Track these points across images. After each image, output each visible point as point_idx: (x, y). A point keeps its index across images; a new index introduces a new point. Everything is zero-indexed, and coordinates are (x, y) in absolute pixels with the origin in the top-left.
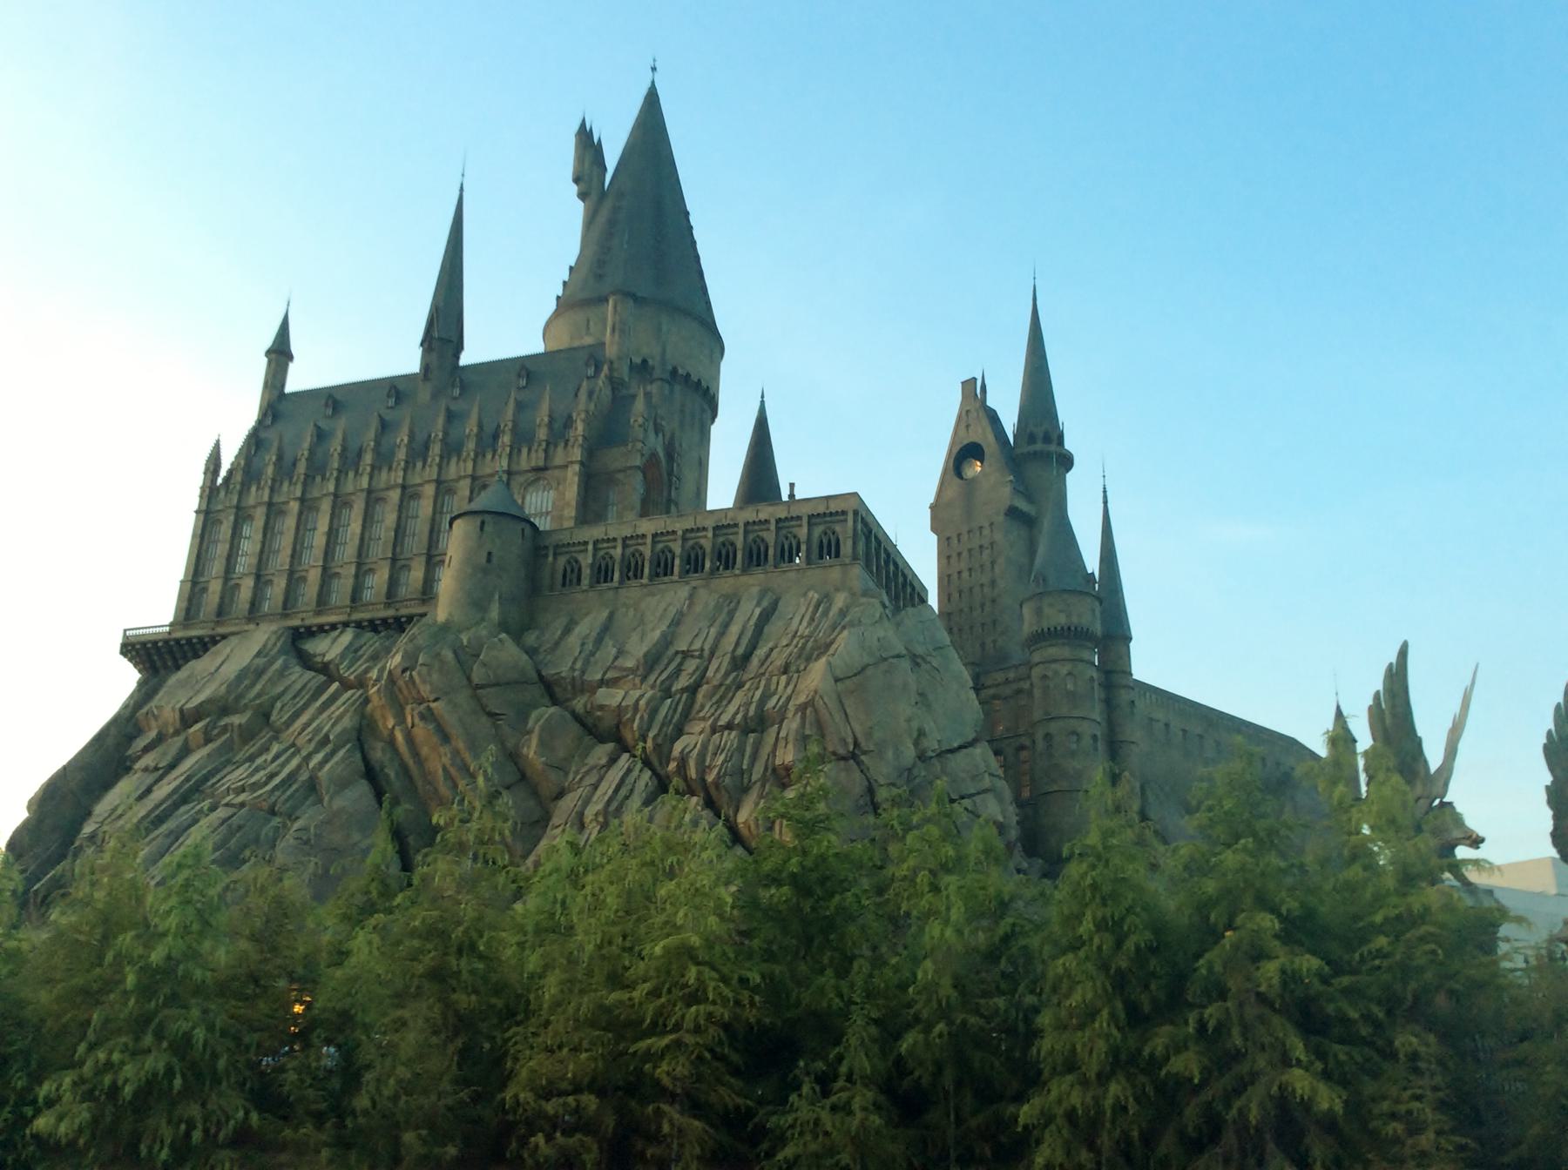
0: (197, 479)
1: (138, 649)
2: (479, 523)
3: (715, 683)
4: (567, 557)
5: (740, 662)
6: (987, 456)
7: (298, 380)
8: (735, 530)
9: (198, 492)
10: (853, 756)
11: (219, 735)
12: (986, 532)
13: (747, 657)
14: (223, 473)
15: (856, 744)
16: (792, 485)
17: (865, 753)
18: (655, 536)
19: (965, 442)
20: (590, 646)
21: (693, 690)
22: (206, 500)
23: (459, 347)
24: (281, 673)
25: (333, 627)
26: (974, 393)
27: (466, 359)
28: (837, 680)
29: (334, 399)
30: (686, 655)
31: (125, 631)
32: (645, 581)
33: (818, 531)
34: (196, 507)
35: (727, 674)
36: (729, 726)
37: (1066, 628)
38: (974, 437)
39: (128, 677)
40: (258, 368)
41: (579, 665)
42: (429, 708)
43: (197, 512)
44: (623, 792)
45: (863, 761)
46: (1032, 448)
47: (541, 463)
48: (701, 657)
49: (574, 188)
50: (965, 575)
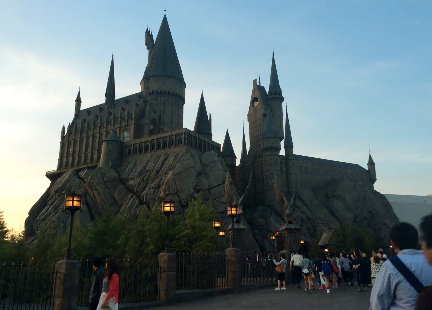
0: (60, 135)
1: (50, 176)
2: (107, 143)
3: (152, 177)
5: (158, 172)
6: (258, 101)
7: (83, 107)
8: (161, 139)
9: (60, 138)
10: (177, 193)
11: (61, 196)
12: (259, 121)
13: (160, 170)
14: (66, 132)
15: (177, 190)
16: (210, 114)
17: (179, 192)
18: (145, 142)
19: (254, 97)
20: (130, 170)
21: (148, 179)
22: (62, 139)
23: (114, 96)
24: (74, 181)
25: (84, 168)
27: (116, 99)
28: (174, 175)
29: (89, 111)
30: (148, 171)
31: (46, 172)
32: (143, 153)
33: (178, 138)
34: (60, 141)
35: (154, 176)
36: (152, 188)
37: (269, 147)
39: (48, 183)
41: (127, 175)
42: (96, 188)
43: (61, 142)
44: (133, 204)
45: (179, 195)
47: (126, 125)
48: (151, 171)
49: (146, 47)
50: (255, 133)
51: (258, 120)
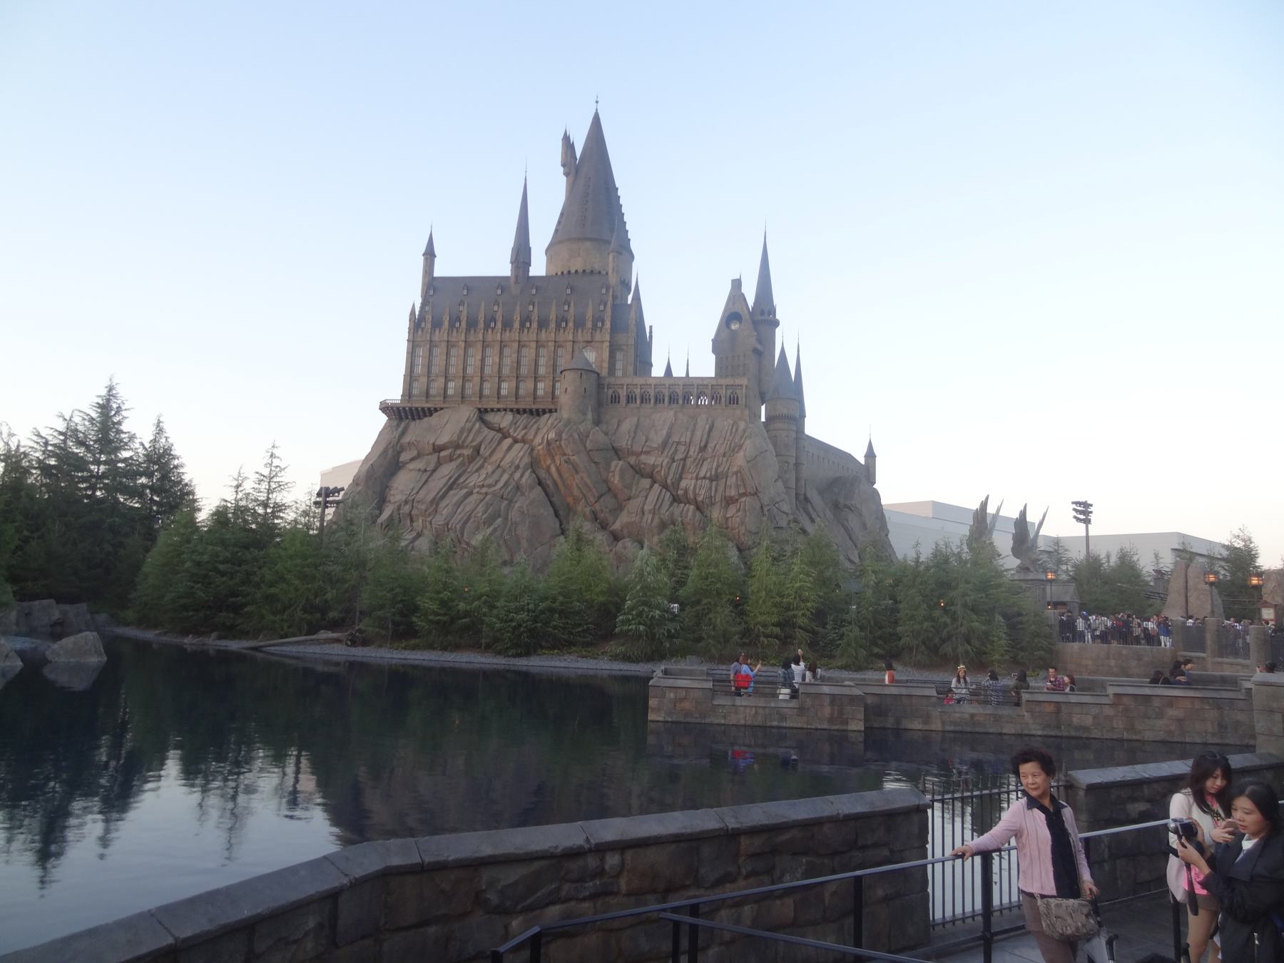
1: (386, 408)
2: (579, 375)
3: (694, 457)
4: (613, 390)
5: (703, 449)
9: (407, 330)
10: (756, 493)
11: (456, 459)
13: (706, 446)
16: (651, 327)
20: (632, 435)
21: (685, 459)
22: (412, 335)
24: (479, 431)
25: (499, 410)
26: (737, 284)
30: (678, 443)
33: (729, 392)
35: (698, 455)
36: (704, 478)
38: (737, 309)
40: (420, 262)
41: (629, 443)
42: (569, 459)
44: (660, 501)
46: (763, 318)
47: (589, 339)
48: (685, 445)
51: (739, 356)
